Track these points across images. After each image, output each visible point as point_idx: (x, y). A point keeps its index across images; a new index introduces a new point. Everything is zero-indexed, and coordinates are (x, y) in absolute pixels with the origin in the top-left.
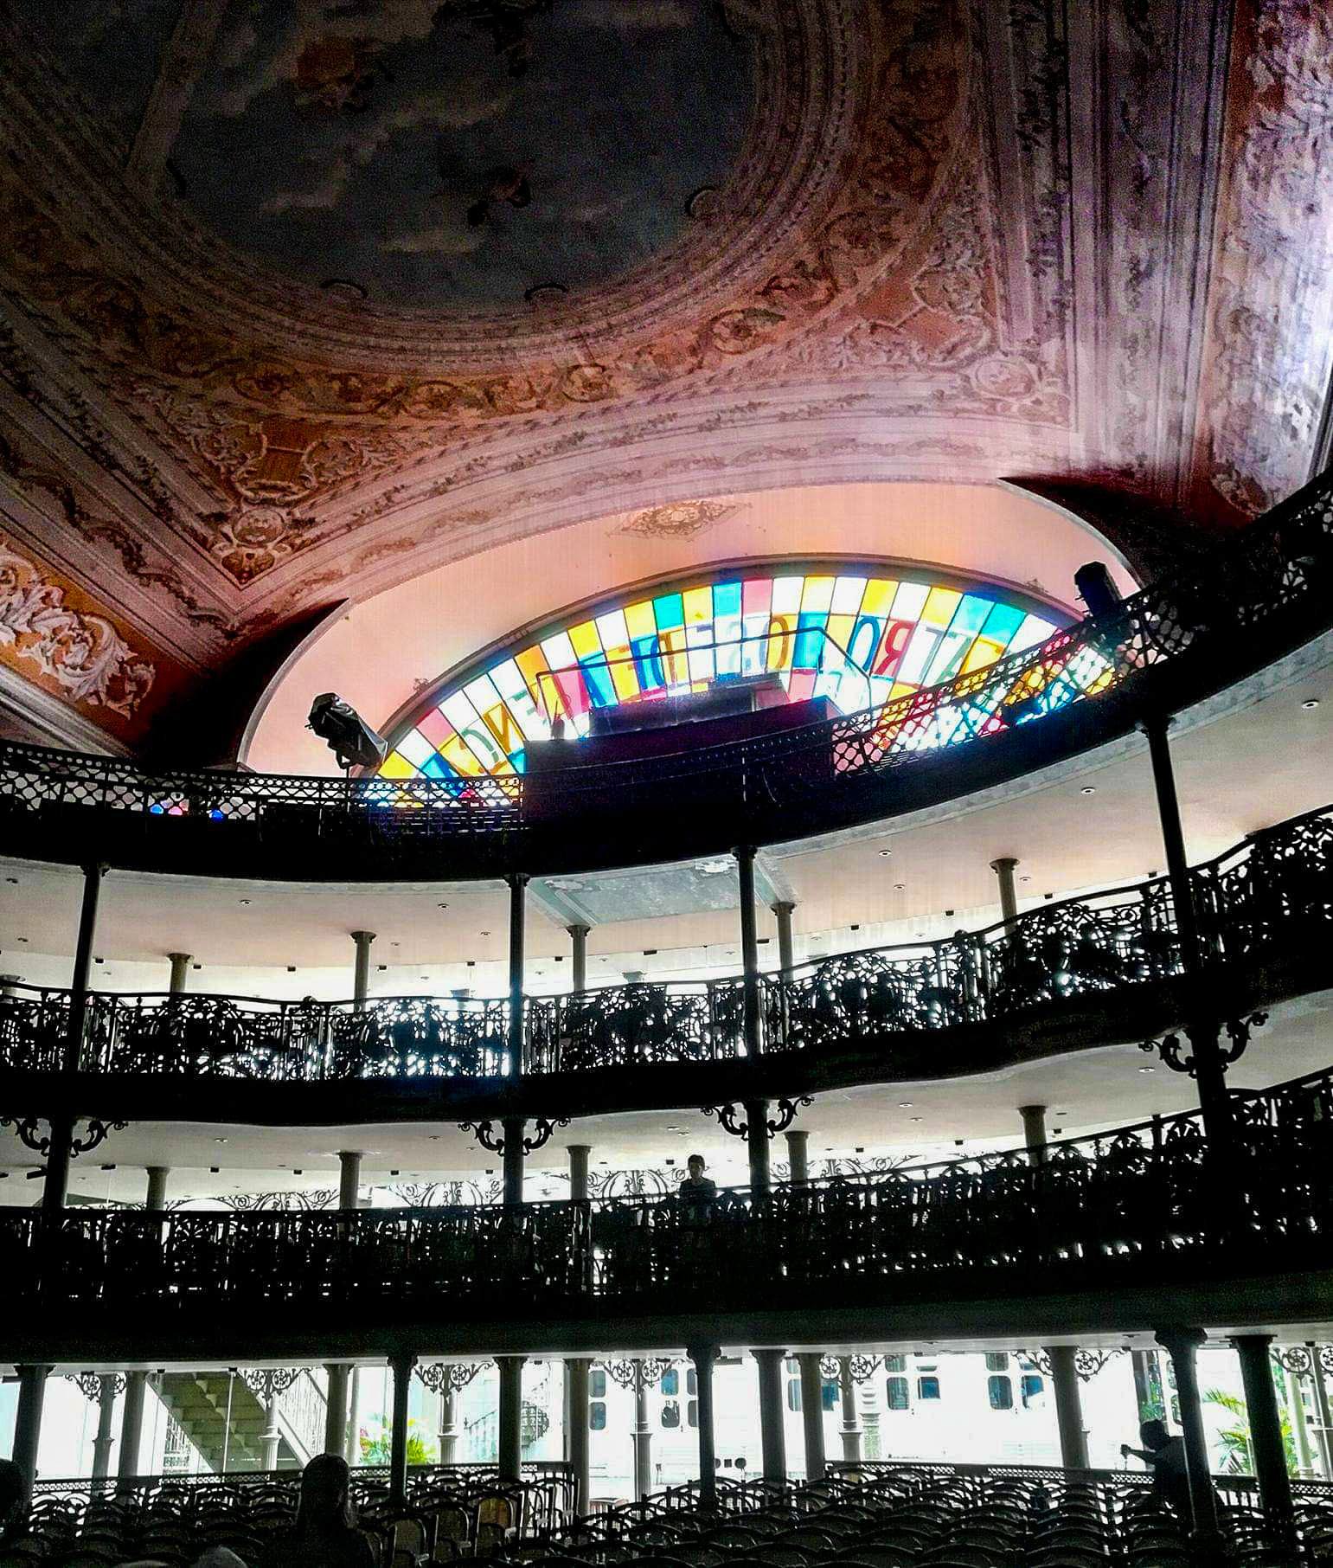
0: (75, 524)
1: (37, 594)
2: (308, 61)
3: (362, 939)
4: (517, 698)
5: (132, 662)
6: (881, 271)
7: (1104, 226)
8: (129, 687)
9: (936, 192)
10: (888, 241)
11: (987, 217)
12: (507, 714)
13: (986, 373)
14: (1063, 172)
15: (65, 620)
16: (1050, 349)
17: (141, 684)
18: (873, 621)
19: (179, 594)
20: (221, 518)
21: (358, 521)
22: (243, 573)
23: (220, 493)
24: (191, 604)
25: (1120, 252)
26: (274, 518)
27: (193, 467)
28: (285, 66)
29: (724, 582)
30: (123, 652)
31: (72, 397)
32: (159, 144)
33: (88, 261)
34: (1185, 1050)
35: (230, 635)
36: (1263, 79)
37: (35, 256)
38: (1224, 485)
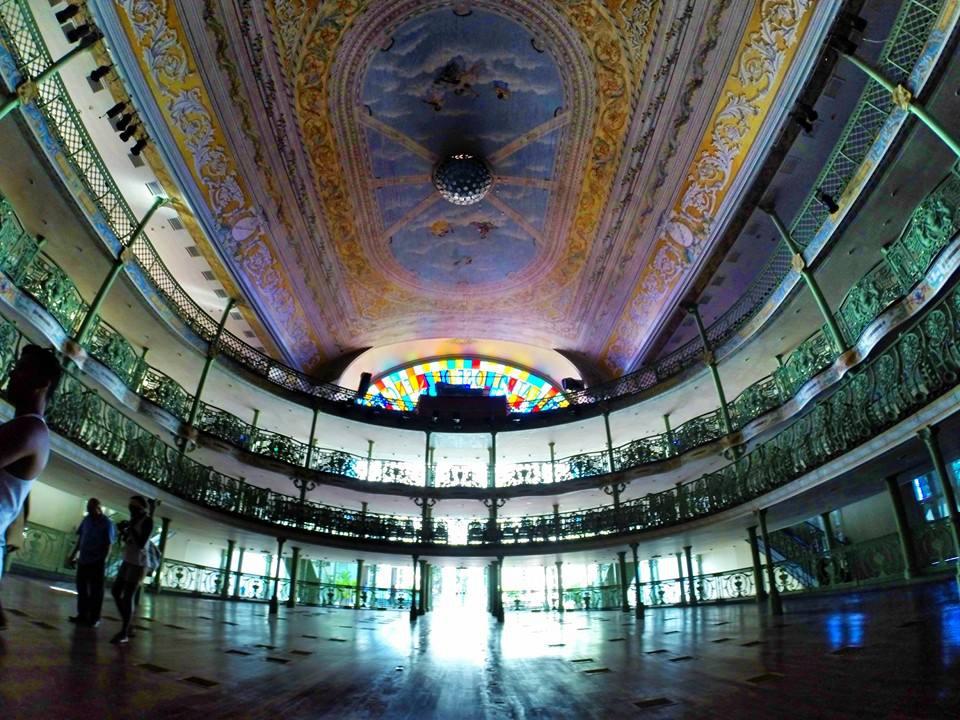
2: (436, 224)
3: (371, 442)
6: (545, 299)
7: (600, 303)
9: (565, 286)
10: (550, 292)
13: (560, 326)
14: (595, 290)
16: (578, 324)
20: (354, 320)
25: (601, 308)
26: (367, 323)
28: (431, 224)
31: (337, 284)
32: (392, 232)
33: (359, 254)
36: (644, 286)
37: (349, 250)
38: (607, 362)
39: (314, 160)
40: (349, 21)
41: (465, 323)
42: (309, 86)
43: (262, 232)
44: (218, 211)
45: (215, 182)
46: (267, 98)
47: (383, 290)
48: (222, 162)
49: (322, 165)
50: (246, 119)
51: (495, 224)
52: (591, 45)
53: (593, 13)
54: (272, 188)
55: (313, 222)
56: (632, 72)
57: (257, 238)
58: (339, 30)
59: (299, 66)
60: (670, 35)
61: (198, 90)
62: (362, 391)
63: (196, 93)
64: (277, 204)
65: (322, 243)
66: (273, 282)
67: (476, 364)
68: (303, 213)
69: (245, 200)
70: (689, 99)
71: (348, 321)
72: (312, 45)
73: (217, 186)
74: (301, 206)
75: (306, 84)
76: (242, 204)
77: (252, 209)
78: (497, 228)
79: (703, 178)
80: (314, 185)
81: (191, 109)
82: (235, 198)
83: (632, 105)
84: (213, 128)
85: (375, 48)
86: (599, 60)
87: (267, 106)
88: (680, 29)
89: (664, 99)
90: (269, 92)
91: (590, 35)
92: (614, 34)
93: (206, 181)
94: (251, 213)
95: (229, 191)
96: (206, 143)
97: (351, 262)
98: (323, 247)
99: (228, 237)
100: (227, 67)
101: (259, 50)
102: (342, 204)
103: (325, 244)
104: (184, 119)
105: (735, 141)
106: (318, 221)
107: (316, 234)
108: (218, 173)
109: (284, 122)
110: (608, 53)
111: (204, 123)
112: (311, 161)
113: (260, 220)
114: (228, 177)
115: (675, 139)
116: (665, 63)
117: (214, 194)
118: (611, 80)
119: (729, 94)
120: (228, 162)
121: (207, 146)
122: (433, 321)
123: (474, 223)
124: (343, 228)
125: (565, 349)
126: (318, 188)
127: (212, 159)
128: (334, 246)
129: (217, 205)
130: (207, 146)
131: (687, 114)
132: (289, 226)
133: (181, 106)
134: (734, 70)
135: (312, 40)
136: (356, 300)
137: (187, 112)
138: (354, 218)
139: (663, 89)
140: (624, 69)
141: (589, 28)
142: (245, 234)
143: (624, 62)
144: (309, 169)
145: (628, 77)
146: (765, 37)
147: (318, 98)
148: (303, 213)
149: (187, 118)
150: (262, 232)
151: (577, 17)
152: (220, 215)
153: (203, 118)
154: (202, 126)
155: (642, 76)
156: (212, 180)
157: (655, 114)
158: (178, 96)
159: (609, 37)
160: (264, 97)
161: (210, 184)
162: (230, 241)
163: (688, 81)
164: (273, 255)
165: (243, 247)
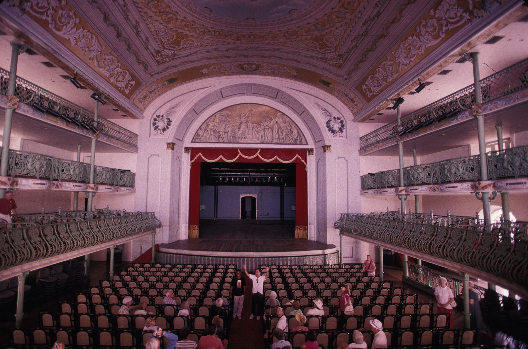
40: (308, 26)
42: (347, 11)
44: (467, 16)
45: (442, 26)
46: (372, 20)
48: (426, 24)
50: (392, 23)
52: (179, 17)
53: (186, 29)
56: (151, 17)
58: (315, 24)
59: (345, 21)
60: (147, 38)
61: (393, 53)
63: (395, 53)
70: (114, 28)
72: (332, 25)
75: (348, 12)
79: (60, 12)
83: (137, 3)
84: (408, 38)
85: (300, 12)
86: (172, 13)
87: (376, 18)
88: (145, 43)
89: (125, 18)
90: (369, 22)
91: (182, 21)
92: (171, 25)
93: (442, 33)
95: (448, 10)
96: (417, 39)
100: (375, 44)
101: (357, 38)
104: (409, 56)
105: (79, 44)
108: (436, 24)
109: (376, 4)
110: (169, 18)
111: (407, 44)
114: (437, 16)
115: (98, 8)
116: (139, 30)
118: (159, 8)
119: (104, 47)
120: (425, 20)
121: (419, 39)
127: (426, 32)
129: (461, 18)
130: (419, 39)
131: (108, 22)
133: (403, 59)
134: (113, 53)
135: (330, 27)
139: (130, 21)
140: (156, 15)
141: (185, 23)
143: (159, 18)
145: (151, 14)
146: (118, 69)
147: (346, 3)
149: (408, 55)
151: (193, 25)
152: (471, 13)
155: (145, 18)
156: (441, 29)
157: (122, 9)
159: (173, 23)
160: (373, 22)
161: (444, 28)
163: (123, 32)
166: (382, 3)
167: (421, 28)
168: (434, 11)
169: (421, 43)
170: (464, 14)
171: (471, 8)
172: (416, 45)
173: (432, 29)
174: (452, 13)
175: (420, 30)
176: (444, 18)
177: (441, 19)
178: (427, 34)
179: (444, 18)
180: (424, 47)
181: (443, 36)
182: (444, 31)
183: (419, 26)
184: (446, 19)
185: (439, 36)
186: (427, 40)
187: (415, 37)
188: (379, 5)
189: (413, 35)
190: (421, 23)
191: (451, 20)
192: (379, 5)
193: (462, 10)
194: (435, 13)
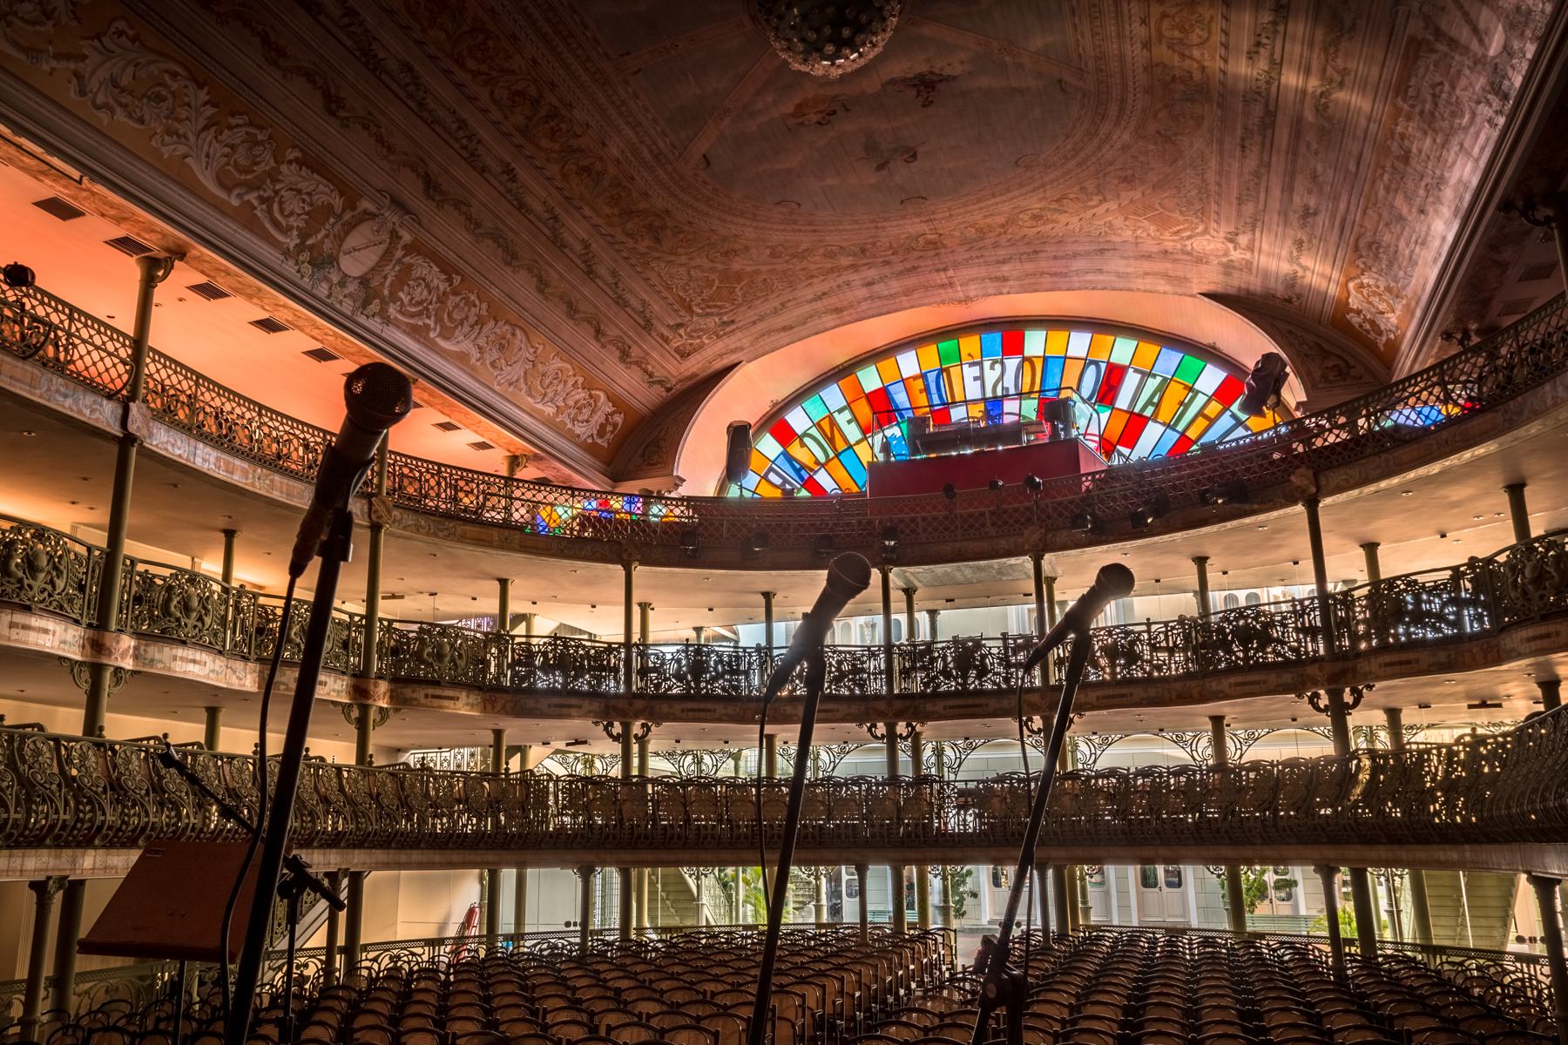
0: (598, 340)
1: (571, 382)
4: (840, 411)
5: (612, 414)
8: (609, 428)
11: (1211, 177)
12: (833, 423)
15: (581, 395)
17: (615, 425)
18: (1096, 363)
19: (646, 371)
20: (680, 325)
21: (762, 318)
22: (684, 354)
23: (682, 313)
24: (651, 375)
26: (712, 322)
27: (671, 300)
29: (990, 331)
30: (609, 408)
31: (614, 273)
32: (702, 146)
33: (643, 206)
34: (1324, 701)
35: (668, 390)
39: (462, 66)
41: (951, 273)
43: (407, 237)
44: (292, 241)
45: (258, 188)
47: (726, 254)
48: (257, 143)
49: (484, 68)
51: (948, 71)
54: (390, 149)
55: (514, 179)
57: (399, 253)
61: (121, 25)
62: (736, 464)
63: (121, 33)
64: (418, 175)
65: (550, 211)
66: (467, 318)
67: (1013, 345)
68: (483, 170)
69: (342, 194)
71: (666, 332)
73: (269, 193)
74: (472, 159)
76: (338, 203)
77: (365, 204)
78: (955, 78)
80: (485, 111)
81: (130, 70)
82: (320, 199)
84: (201, 86)
93: (239, 196)
94: (365, 212)
95: (299, 191)
96: (202, 122)
97: (629, 225)
98: (555, 218)
99: (335, 278)
102: (563, 126)
103: (558, 210)
106: (522, 173)
107: (530, 201)
108: (259, 169)
109: (356, 13)
111: (175, 86)
112: (455, 69)
113: (392, 217)
114: (284, 168)
117: (270, 211)
120: (270, 137)
121: (206, 128)
122: (869, 284)
123: (893, 82)
124: (587, 170)
125: (1232, 291)
126: (496, 115)
127: (233, 147)
128: (578, 209)
129: (286, 231)
130: (206, 128)
132: (458, 204)
133: (102, 74)
136: (669, 288)
137: (125, 80)
138: (604, 145)
142: (370, 258)
144: (459, 86)
148: (483, 170)
150: (407, 237)
152: (300, 248)
153: (167, 77)
154: (173, 94)
156: (251, 187)
158: (85, 57)
161: (252, 197)
162: (342, 284)
164: (447, 269)
165: (375, 283)
166: (352, 29)
167: (244, 130)
168: (296, 160)
169: (190, 135)
170: (295, 233)
171: (310, 242)
172: (180, 121)
173: (243, 162)
174: (293, 205)
175: (237, 126)
176: (278, 187)
177: (275, 181)
178: (227, 150)
179: (278, 187)
180: (182, 149)
181: (235, 202)
182: (246, 198)
183: (251, 124)
184: (276, 192)
185: (229, 191)
186: (208, 156)
187: (210, 111)
188: (346, 20)
189: (215, 105)
190: (262, 128)
191: (276, 206)
192: (346, 20)
193: (302, 224)
194: (290, 162)
